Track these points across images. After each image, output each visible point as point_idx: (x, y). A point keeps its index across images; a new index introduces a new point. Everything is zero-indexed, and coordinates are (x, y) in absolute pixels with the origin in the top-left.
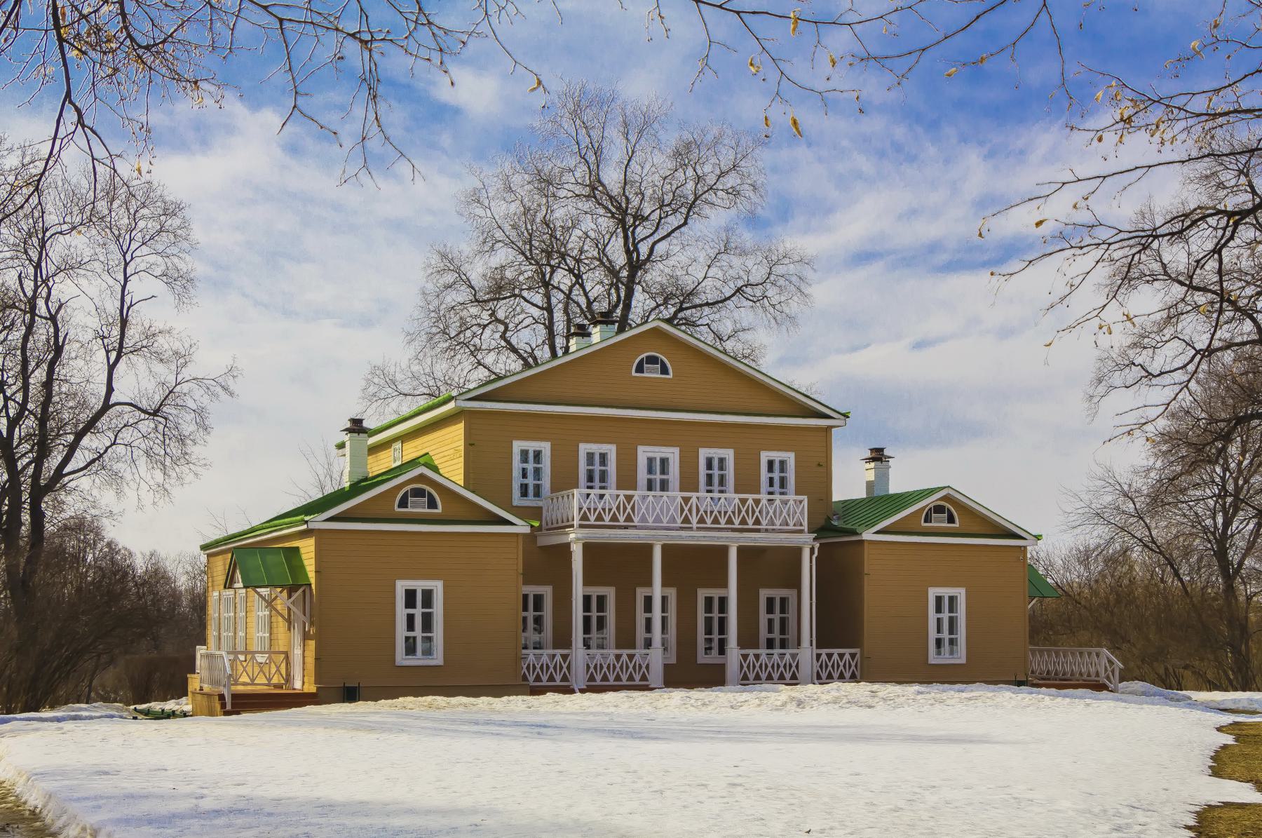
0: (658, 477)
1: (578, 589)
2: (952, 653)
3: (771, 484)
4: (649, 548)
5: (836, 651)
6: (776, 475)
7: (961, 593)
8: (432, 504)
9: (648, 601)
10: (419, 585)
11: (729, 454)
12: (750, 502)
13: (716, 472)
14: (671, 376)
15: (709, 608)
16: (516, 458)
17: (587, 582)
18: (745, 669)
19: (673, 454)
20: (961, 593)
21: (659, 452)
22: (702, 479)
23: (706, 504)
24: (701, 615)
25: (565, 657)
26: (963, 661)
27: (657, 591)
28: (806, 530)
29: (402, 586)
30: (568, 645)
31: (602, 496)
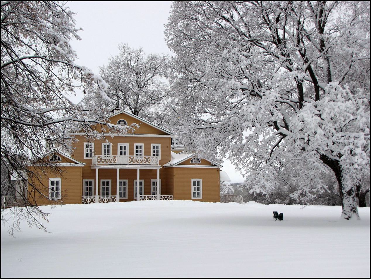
1: (118, 180)
2: (198, 196)
5: (166, 196)
9: (136, 183)
12: (147, 158)
13: (139, 149)
17: (120, 179)
25: (115, 197)
26: (202, 198)
27: (138, 180)
28: (158, 164)
30: (115, 194)
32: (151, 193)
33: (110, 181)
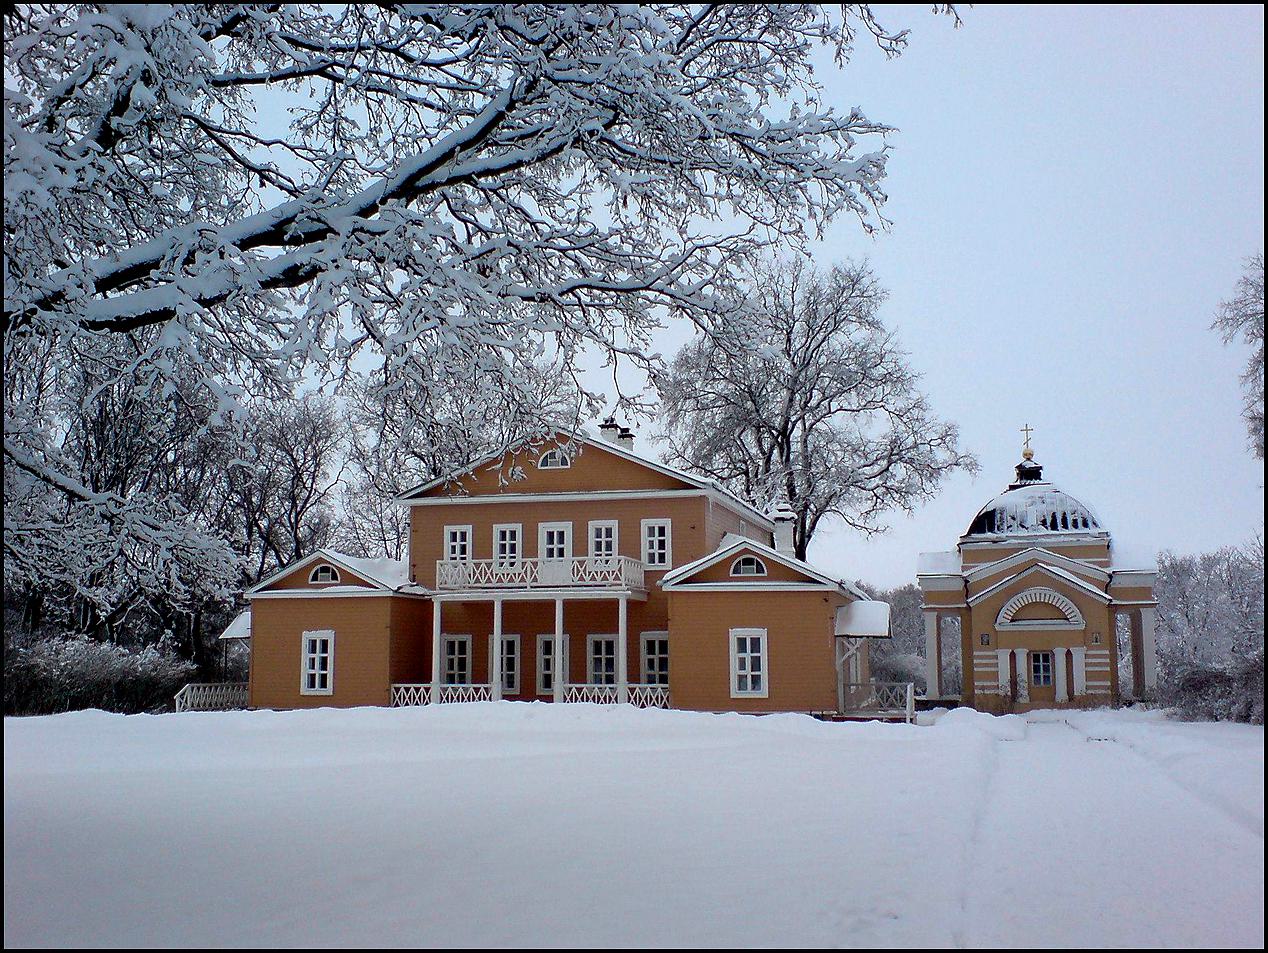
0: (556, 546)
3: (454, 552)
4: (553, 603)
6: (458, 544)
7: (762, 634)
8: (760, 569)
9: (548, 648)
10: (748, 633)
11: (614, 524)
14: (569, 467)
15: (598, 650)
16: (644, 531)
18: (427, 697)
19: (567, 527)
20: (762, 634)
21: (556, 527)
22: (591, 546)
23: (601, 567)
24: (590, 656)
29: (735, 633)
31: (607, 562)
32: (643, 677)
33: (468, 638)
